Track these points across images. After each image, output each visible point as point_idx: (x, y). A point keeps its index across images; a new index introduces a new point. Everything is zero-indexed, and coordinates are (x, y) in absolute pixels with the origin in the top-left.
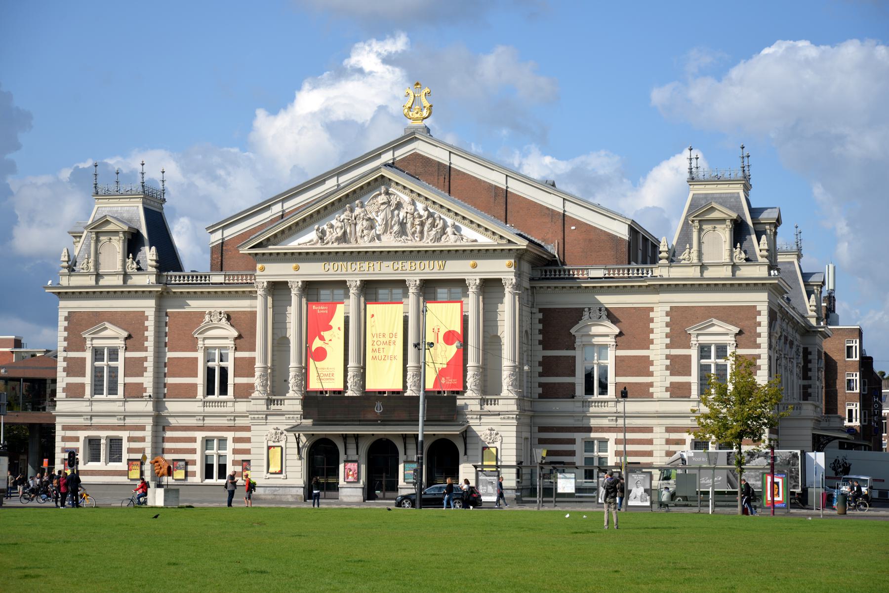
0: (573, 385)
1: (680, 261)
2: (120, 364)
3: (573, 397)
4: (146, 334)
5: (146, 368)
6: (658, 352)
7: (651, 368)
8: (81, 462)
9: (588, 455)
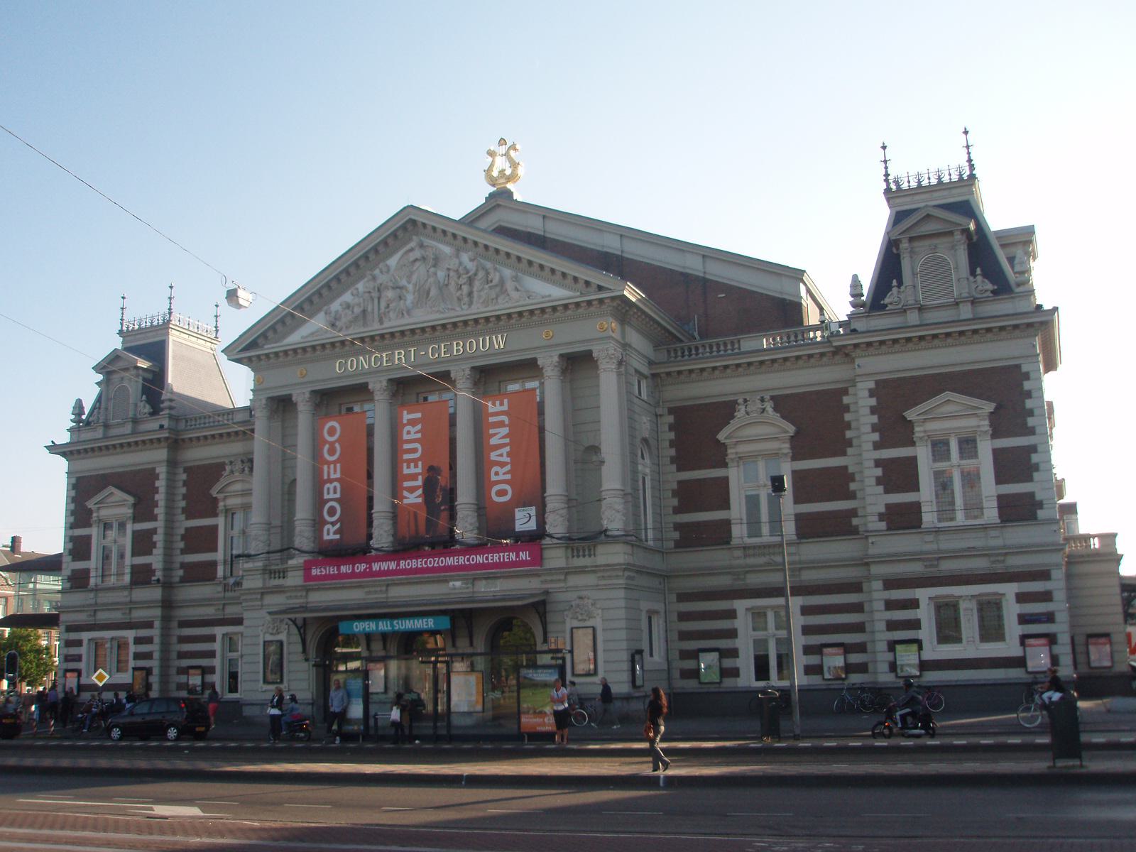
0: (727, 524)
1: (886, 306)
3: (728, 543)
8: (84, 674)
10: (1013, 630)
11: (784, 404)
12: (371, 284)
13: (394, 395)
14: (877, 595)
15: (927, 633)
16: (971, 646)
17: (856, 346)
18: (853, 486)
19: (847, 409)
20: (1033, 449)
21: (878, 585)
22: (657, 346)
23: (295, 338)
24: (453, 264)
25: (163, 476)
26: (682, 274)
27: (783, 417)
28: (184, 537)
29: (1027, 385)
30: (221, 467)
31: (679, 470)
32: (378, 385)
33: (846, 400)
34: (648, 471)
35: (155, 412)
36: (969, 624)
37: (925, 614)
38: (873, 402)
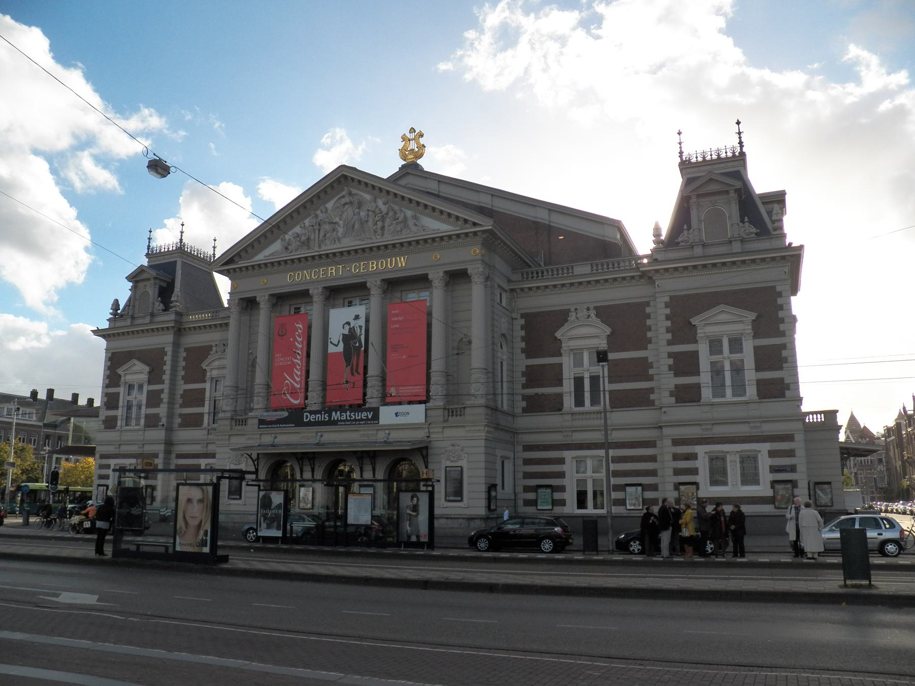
2: (143, 398)
3: (560, 410)
4: (165, 368)
6: (659, 351)
9: (581, 476)
10: (766, 477)
11: (604, 313)
12: (314, 221)
13: (327, 299)
14: (666, 450)
15: (703, 478)
16: (734, 488)
17: (657, 271)
18: (651, 372)
19: (648, 316)
20: (784, 346)
21: (669, 442)
22: (514, 269)
23: (260, 257)
24: (372, 206)
25: (169, 353)
26: (534, 222)
27: (602, 321)
29: (780, 301)
30: (209, 348)
31: (527, 358)
32: (316, 292)
33: (648, 310)
34: (505, 357)
35: (166, 309)
36: (734, 471)
37: (702, 464)
38: (668, 311)
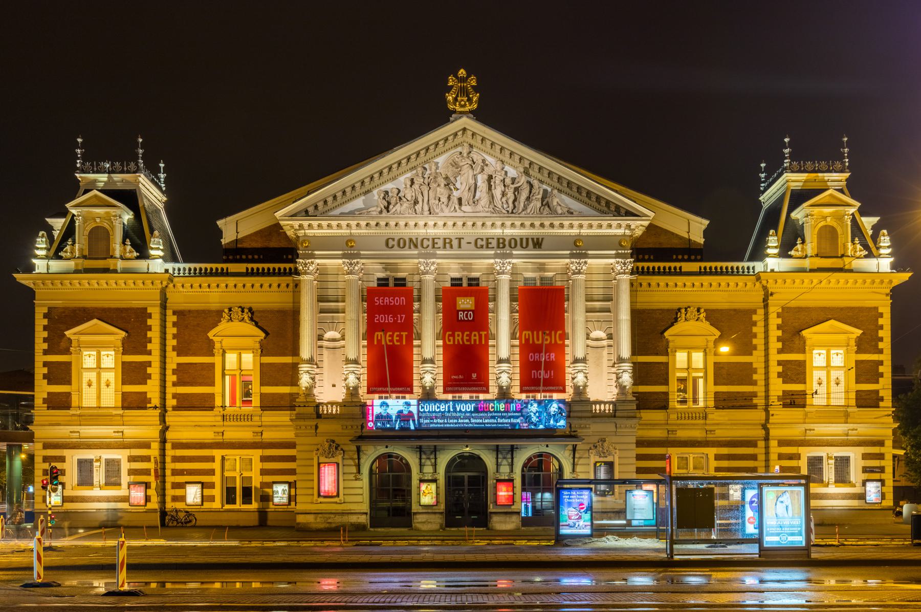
5: (150, 375)
7: (755, 377)
8: (68, 486)
28: (174, 372)
